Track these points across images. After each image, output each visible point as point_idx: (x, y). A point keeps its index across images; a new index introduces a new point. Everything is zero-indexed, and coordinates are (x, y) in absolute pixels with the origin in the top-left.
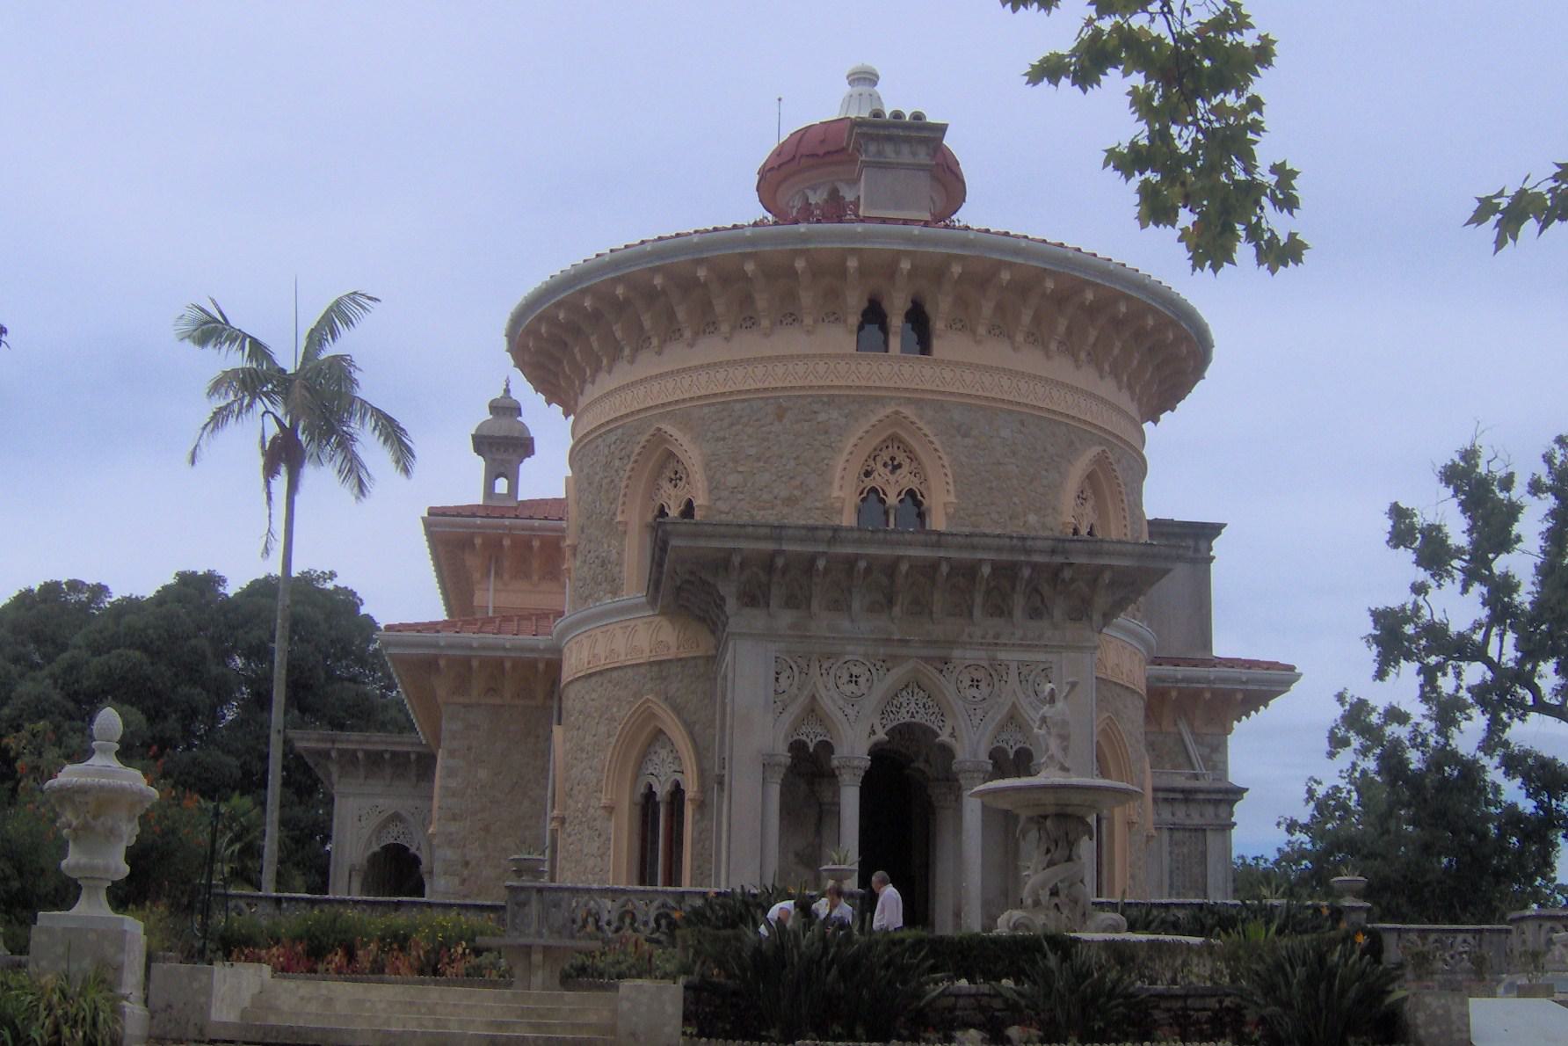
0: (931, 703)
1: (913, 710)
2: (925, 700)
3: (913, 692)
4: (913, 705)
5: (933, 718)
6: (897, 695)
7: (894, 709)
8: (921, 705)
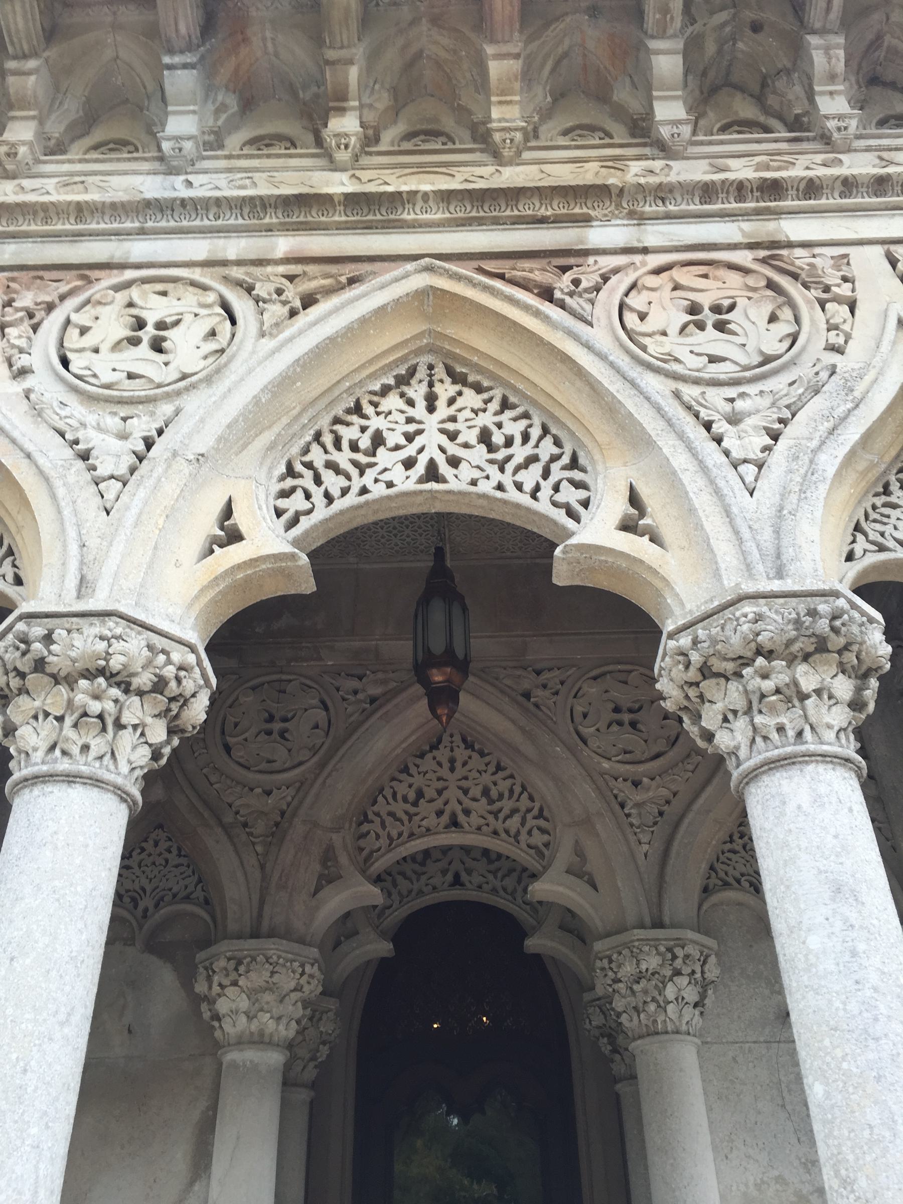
0: (504, 786)
1: (454, 806)
2: (486, 778)
3: (452, 761)
4: (453, 793)
5: (514, 823)
6: (406, 770)
7: (399, 808)
8: (476, 791)
